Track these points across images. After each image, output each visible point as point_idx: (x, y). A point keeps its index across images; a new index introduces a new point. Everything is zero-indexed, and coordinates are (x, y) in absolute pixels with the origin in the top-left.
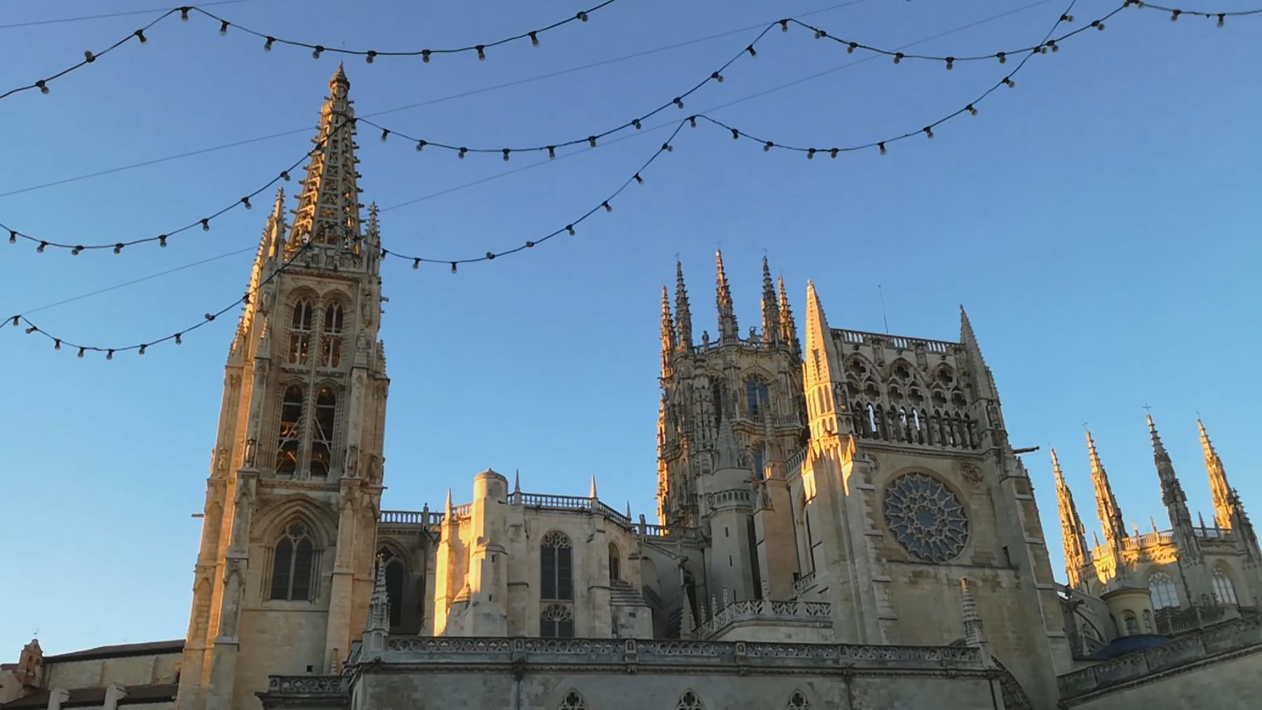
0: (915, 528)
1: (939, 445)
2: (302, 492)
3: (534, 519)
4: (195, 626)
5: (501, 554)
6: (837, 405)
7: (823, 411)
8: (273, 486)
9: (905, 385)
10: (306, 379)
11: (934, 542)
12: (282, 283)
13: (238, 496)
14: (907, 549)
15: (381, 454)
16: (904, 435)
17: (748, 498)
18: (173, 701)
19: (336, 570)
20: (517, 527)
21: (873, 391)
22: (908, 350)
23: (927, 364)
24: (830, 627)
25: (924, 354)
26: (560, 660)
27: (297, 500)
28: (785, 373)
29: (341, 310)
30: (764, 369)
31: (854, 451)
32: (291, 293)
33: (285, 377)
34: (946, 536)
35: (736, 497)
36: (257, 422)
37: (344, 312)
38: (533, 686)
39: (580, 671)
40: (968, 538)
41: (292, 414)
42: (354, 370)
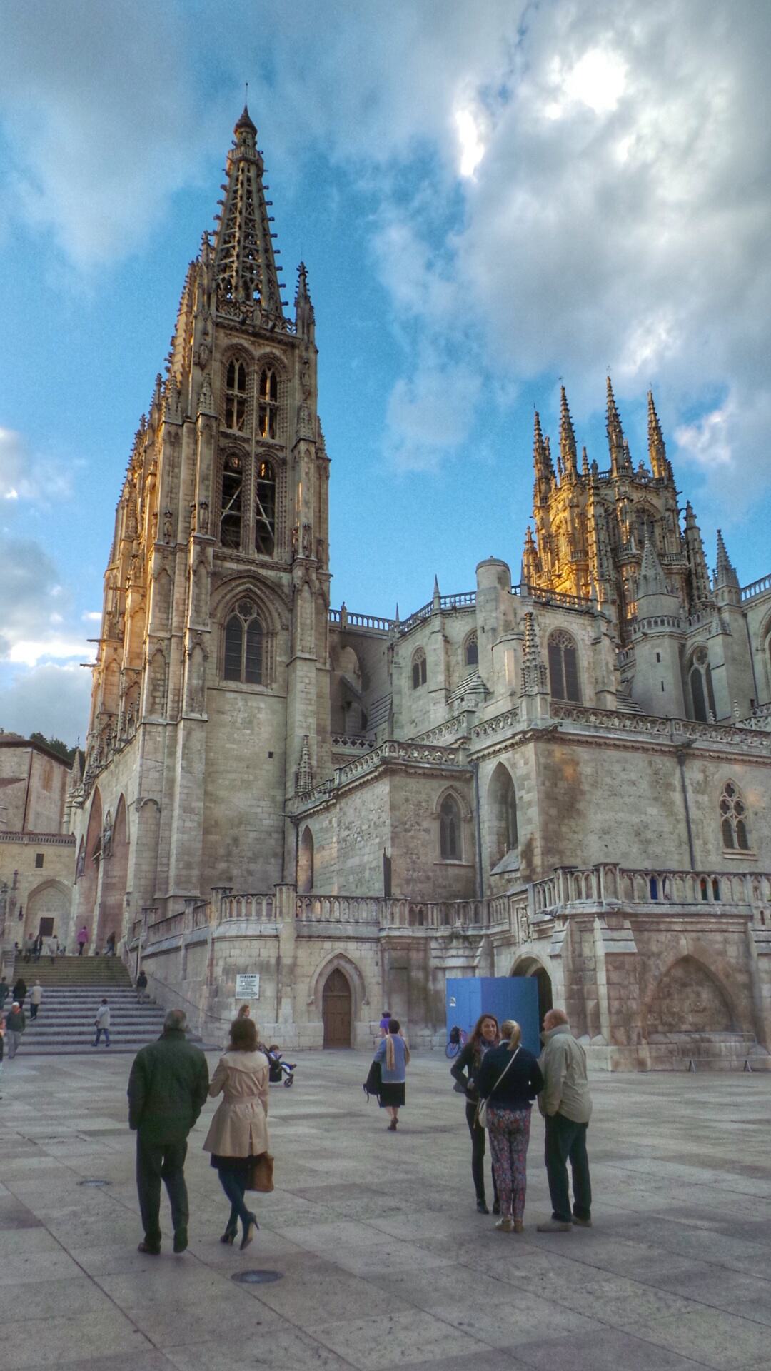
2: (253, 568)
3: (541, 615)
4: (151, 700)
8: (224, 559)
10: (246, 446)
12: (217, 338)
13: (196, 563)
15: (327, 539)
17: (679, 626)
26: (715, 747)
27: (248, 577)
29: (275, 378)
30: (652, 505)
32: (226, 351)
33: (224, 442)
35: (669, 623)
36: (208, 486)
37: (278, 379)
38: (694, 772)
41: (230, 486)
42: (302, 443)
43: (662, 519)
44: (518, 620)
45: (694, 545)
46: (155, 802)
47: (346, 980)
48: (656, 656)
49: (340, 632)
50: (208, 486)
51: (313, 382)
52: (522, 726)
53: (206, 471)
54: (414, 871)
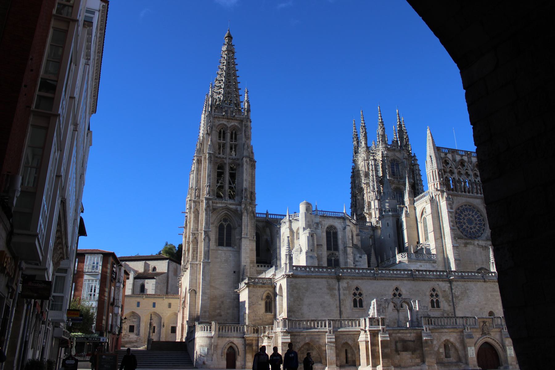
0: (466, 226)
1: (475, 194)
4: (192, 255)
5: (315, 234)
6: (440, 178)
7: (434, 180)
8: (217, 203)
9: (464, 170)
11: (473, 231)
14: (463, 233)
15: (255, 191)
16: (463, 190)
18: (155, 279)
19: (243, 236)
20: (317, 224)
21: (452, 172)
22: (465, 155)
23: (471, 161)
24: (436, 263)
25: (471, 157)
28: (406, 159)
31: (446, 196)
32: (218, 126)
34: (477, 229)
36: (210, 178)
39: (359, 279)
40: (485, 230)
41: (220, 175)
42: (244, 158)
43: (402, 162)
44: (314, 224)
45: (416, 172)
46: (194, 290)
47: (234, 349)
48: (387, 224)
49: (266, 222)
50: (210, 178)
51: (249, 133)
52: (284, 273)
53: (210, 173)
54: (256, 317)
